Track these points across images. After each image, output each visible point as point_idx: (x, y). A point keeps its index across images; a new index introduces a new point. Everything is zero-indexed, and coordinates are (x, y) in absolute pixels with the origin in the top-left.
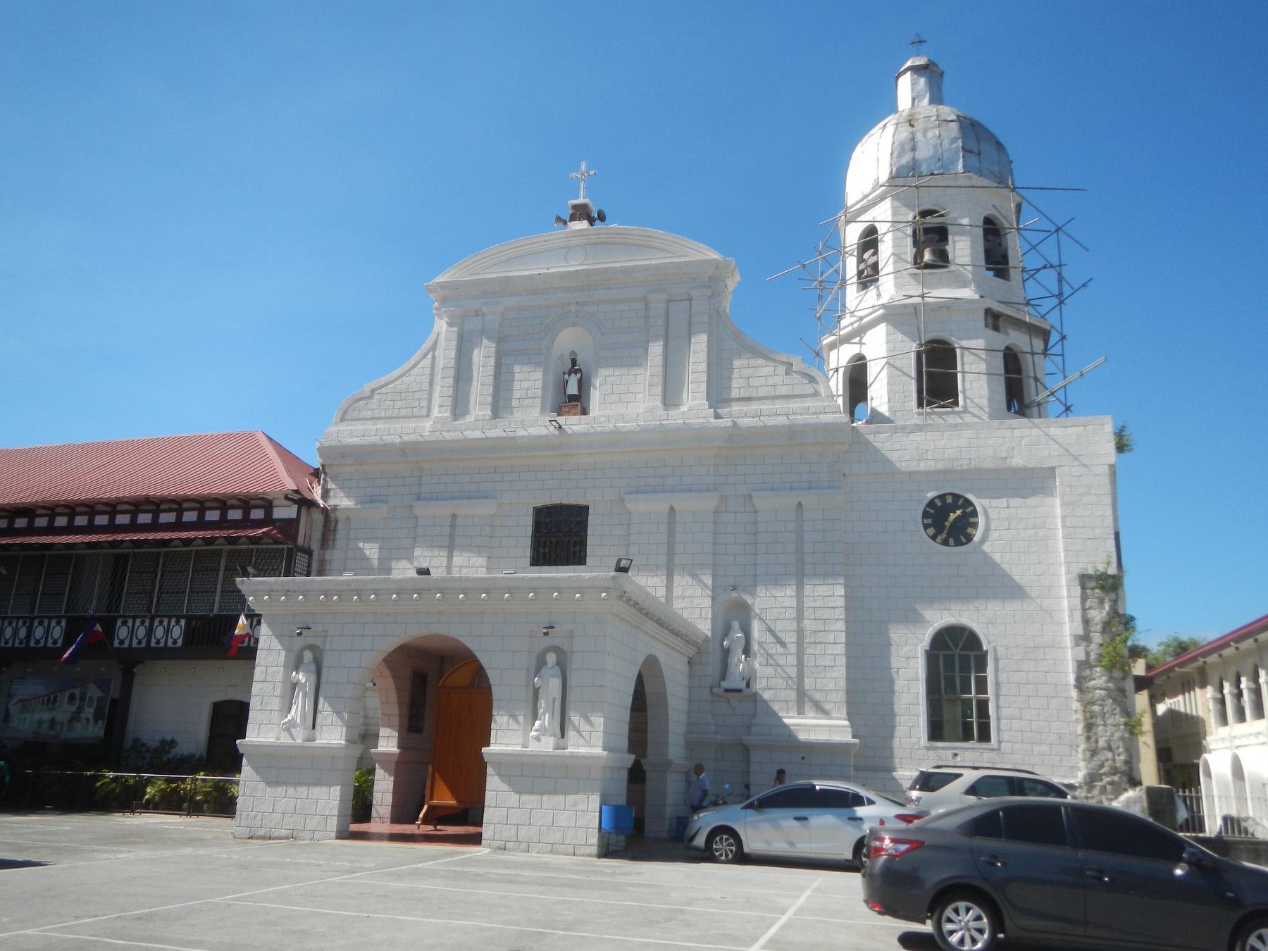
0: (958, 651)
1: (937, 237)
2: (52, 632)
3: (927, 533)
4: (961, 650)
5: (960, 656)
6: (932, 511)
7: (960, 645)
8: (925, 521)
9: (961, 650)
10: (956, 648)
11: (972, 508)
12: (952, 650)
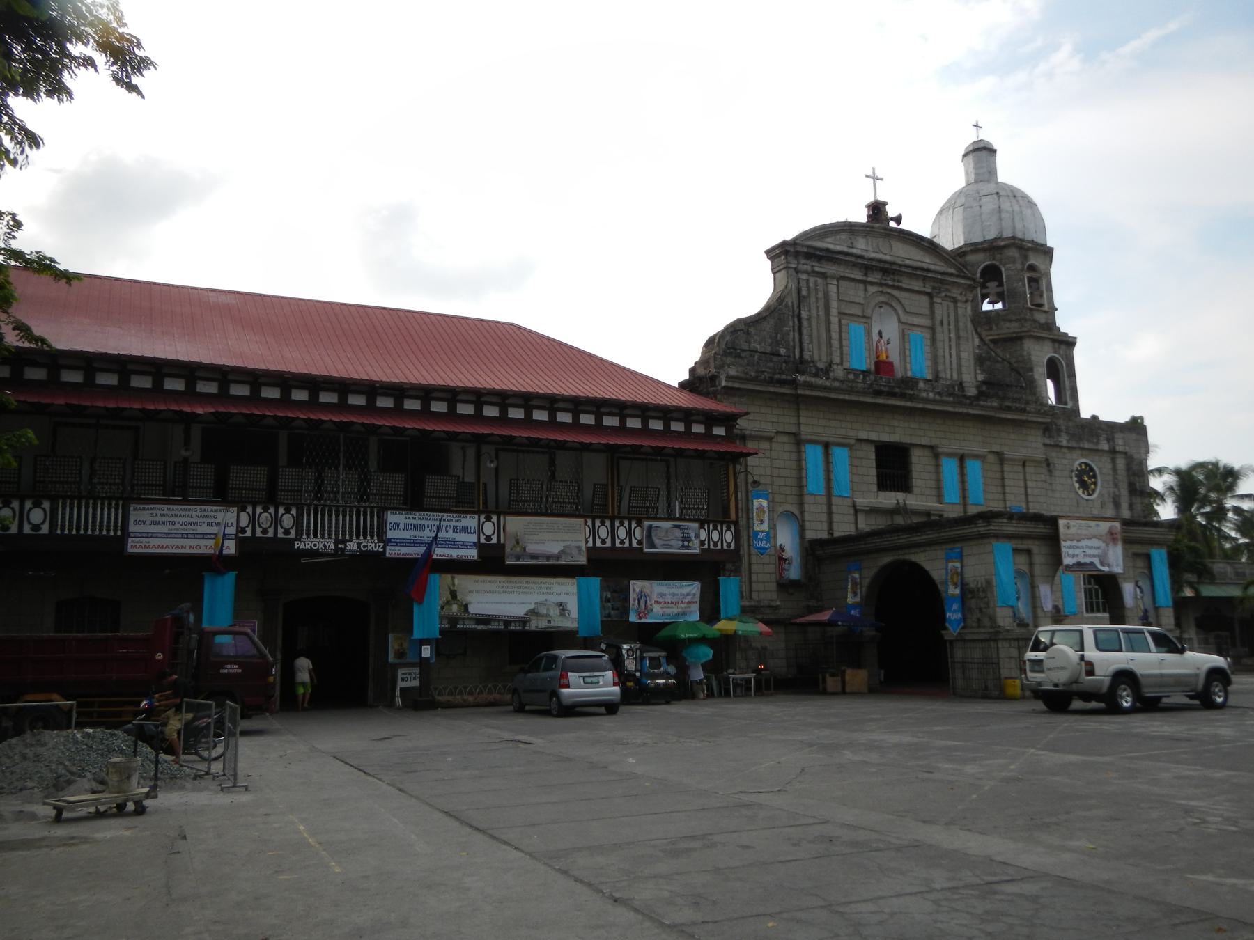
2: (281, 521)
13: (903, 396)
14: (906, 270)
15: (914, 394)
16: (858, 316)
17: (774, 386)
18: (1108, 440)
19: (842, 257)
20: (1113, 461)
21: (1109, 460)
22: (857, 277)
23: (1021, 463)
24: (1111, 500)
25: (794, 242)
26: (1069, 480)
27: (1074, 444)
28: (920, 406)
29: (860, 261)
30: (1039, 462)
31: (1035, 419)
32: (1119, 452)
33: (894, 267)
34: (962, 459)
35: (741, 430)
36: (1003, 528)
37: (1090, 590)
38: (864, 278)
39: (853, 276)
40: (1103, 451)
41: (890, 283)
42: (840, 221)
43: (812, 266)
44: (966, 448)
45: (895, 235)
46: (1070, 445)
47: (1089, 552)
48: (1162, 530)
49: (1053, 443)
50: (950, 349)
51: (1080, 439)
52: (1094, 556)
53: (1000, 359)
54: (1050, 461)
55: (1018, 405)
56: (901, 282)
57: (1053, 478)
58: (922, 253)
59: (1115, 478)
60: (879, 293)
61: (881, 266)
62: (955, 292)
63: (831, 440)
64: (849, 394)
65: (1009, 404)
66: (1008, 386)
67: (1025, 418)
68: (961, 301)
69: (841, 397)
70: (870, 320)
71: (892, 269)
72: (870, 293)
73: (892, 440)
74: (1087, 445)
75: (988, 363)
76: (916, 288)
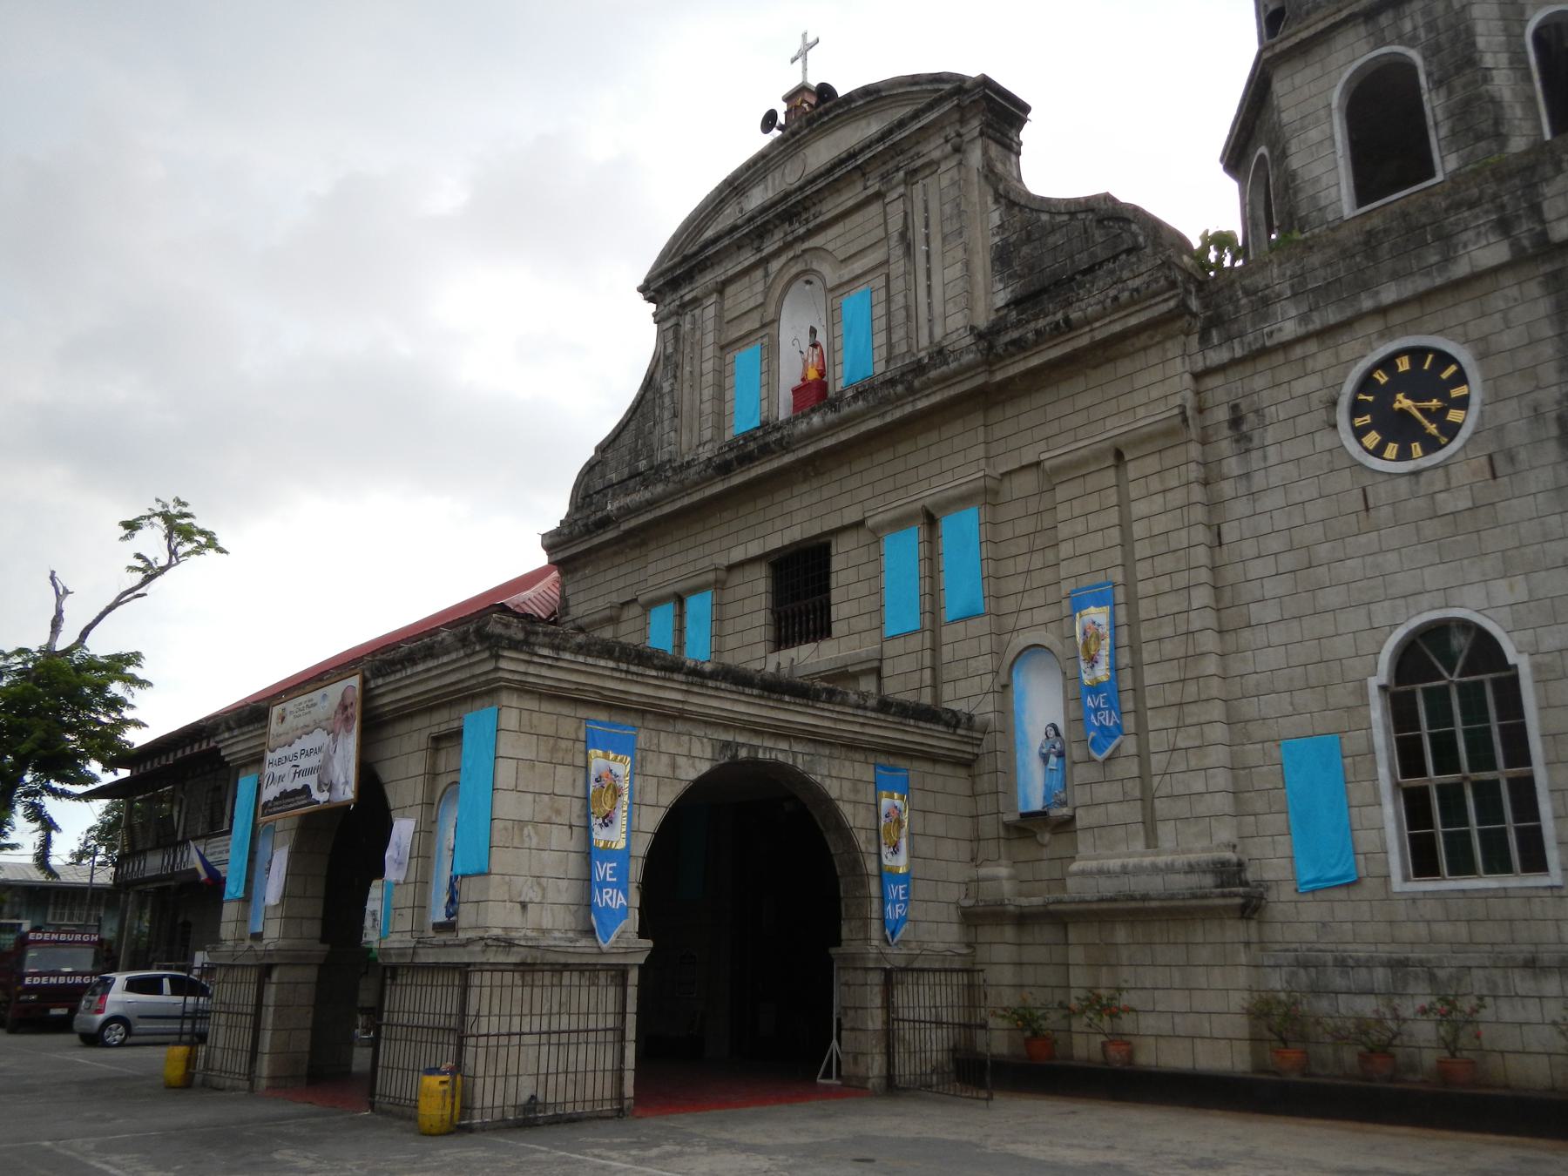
0: (1453, 679)
3: (1361, 443)
4: (1461, 675)
5: (1462, 687)
6: (1370, 398)
7: (1460, 663)
8: (1358, 422)
9: (1461, 675)
10: (1451, 674)
11: (1453, 368)
12: (1443, 678)
13: (766, 451)
14: (815, 189)
15: (782, 438)
16: (756, 330)
17: (598, 535)
18: (1504, 226)
19: (711, 251)
21: (1533, 289)
22: (746, 264)
23: (1111, 461)
24: (1554, 430)
25: (648, 281)
26: (1324, 440)
27: (1332, 316)
28: (810, 450)
29: (737, 235)
30: (1169, 433)
33: (793, 200)
34: (930, 520)
35: (573, 620)
36: (235, 749)
38: (758, 256)
39: (739, 268)
40: (1496, 270)
41: (802, 231)
42: (708, 192)
43: (682, 297)
44: (927, 494)
45: (805, 136)
46: (1317, 323)
47: (304, 763)
48: (454, 656)
49: (1239, 353)
50: (929, 277)
51: (1366, 286)
53: (1065, 218)
54: (1244, 407)
55: (1041, 323)
56: (821, 214)
57: (1255, 455)
58: (863, 123)
60: (791, 263)
61: (771, 215)
62: (934, 148)
63: (678, 587)
64: (688, 495)
65: (1015, 334)
66: (1084, 272)
67: (1084, 341)
68: (946, 158)
69: (678, 505)
70: (776, 325)
71: (793, 205)
72: (772, 276)
74: (1389, 294)
75: (1025, 250)
76: (850, 203)
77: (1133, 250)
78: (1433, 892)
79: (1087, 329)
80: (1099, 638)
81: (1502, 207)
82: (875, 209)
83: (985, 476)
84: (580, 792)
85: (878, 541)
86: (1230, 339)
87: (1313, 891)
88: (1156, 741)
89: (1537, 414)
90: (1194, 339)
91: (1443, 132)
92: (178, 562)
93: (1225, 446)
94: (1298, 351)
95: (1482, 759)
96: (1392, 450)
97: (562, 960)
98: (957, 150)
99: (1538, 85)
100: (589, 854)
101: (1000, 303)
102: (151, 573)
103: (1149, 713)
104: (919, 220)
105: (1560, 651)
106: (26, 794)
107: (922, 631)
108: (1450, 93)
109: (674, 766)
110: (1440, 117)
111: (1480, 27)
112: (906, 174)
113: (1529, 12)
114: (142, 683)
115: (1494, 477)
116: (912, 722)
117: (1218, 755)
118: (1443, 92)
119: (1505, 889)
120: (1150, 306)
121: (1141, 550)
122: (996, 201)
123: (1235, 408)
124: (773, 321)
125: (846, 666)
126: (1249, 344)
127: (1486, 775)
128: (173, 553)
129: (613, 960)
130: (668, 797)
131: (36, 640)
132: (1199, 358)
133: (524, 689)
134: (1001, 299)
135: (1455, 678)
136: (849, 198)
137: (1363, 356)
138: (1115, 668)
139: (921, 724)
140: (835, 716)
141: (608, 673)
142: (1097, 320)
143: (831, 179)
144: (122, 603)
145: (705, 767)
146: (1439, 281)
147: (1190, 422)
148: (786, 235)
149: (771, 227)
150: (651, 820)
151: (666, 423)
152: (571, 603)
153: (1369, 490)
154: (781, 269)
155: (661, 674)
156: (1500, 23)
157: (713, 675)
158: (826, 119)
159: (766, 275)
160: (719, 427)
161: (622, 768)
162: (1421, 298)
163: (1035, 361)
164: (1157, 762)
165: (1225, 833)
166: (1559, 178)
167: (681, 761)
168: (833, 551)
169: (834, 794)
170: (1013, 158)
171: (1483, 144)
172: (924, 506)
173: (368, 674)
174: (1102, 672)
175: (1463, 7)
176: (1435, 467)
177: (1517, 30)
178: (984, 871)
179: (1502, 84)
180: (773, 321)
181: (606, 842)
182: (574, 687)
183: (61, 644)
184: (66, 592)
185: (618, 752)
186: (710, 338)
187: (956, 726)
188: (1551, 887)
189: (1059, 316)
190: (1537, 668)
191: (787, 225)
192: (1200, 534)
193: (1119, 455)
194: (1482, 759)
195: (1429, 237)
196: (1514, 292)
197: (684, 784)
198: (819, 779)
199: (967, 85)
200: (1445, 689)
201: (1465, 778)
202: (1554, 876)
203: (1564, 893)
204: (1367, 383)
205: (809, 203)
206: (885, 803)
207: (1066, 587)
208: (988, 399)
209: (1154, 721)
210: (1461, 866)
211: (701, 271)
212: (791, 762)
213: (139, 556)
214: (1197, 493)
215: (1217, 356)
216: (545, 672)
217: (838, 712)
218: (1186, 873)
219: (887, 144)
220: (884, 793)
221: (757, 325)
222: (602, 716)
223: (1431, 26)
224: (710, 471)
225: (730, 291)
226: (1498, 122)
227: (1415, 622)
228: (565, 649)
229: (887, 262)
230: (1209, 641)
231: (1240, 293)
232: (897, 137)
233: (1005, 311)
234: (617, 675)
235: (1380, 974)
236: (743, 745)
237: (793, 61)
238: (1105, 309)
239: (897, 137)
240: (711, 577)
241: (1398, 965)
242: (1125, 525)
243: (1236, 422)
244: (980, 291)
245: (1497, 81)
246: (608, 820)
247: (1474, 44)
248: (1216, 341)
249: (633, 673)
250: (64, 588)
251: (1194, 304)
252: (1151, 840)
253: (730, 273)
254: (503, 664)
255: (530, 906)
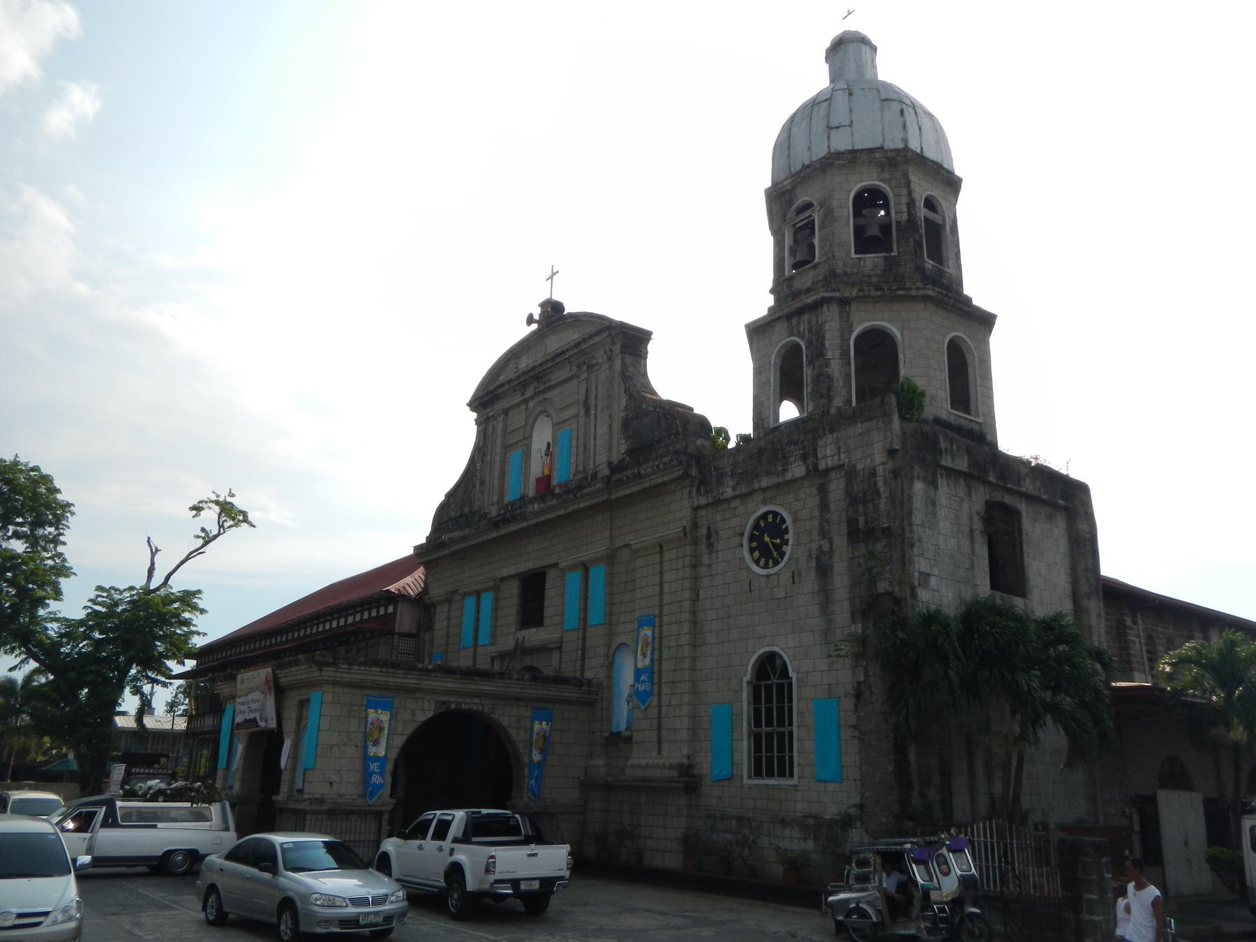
1: (808, 232)
3: (752, 556)
4: (778, 679)
6: (757, 533)
18: (804, 457)
19: (500, 391)
20: (823, 490)
21: (814, 491)
23: (658, 549)
24: (814, 564)
27: (743, 489)
28: (534, 521)
31: (660, 481)
32: (827, 471)
34: (586, 569)
37: (769, 736)
39: (514, 402)
41: (542, 388)
46: (738, 493)
51: (756, 476)
52: (255, 711)
57: (714, 555)
59: (823, 520)
67: (647, 485)
73: (526, 569)
74: (764, 483)
76: (564, 377)
77: (677, 434)
78: (758, 785)
79: (648, 479)
80: (647, 644)
81: (804, 448)
82: (574, 383)
83: (606, 549)
84: (362, 730)
85: (564, 575)
86: (707, 492)
87: (717, 781)
88: (665, 700)
89: (810, 556)
90: (694, 490)
91: (809, 390)
92: (224, 532)
93: (704, 549)
94: (733, 504)
95: (781, 724)
96: (762, 561)
97: (349, 808)
98: (609, 359)
99: (853, 368)
100: (366, 759)
101: (623, 451)
102: (208, 539)
103: (663, 685)
104: (593, 397)
105: (807, 672)
106: (132, 681)
107: (579, 629)
108: (813, 370)
109: (413, 715)
110: (809, 381)
111: (828, 335)
112: (588, 367)
113: (855, 326)
114: (202, 611)
115: (794, 583)
116: (553, 685)
117: (685, 710)
118: (811, 367)
119: (780, 785)
120: (672, 472)
121: (666, 599)
122: (625, 392)
123: (709, 528)
124: (529, 437)
125: (546, 644)
126: (714, 497)
127: (781, 729)
128: (221, 526)
129: (375, 809)
130: (409, 730)
131: (140, 582)
132: (696, 499)
133: (334, 683)
134: (623, 448)
135: (775, 681)
136: (563, 374)
137: (755, 512)
138: (652, 660)
139: (559, 686)
140: (505, 685)
141: (377, 673)
142: (652, 475)
143: (554, 363)
144: (190, 558)
145: (430, 714)
146: (781, 480)
147: (688, 534)
148: (536, 388)
149: (528, 382)
150: (399, 742)
151: (477, 488)
152: (429, 587)
153: (752, 581)
154: (534, 407)
155: (405, 672)
156: (839, 332)
157: (433, 670)
158: (554, 325)
159: (527, 409)
160: (501, 495)
161: (385, 717)
162: (777, 486)
163: (628, 492)
164: (664, 709)
165: (685, 751)
166: (824, 438)
167: (418, 712)
168: (547, 578)
169: (505, 724)
170: (642, 361)
171: (821, 400)
172: (582, 561)
173: (274, 668)
174: (647, 661)
175: (822, 323)
176: (774, 574)
177: (847, 337)
178: (594, 762)
179: (835, 368)
180: (529, 437)
181: (375, 753)
182: (359, 681)
183: (153, 586)
184: (157, 550)
185: (383, 709)
186: (499, 441)
187: (581, 685)
188: (794, 785)
189: (636, 470)
190: (799, 680)
191: (536, 382)
192: (687, 595)
193: (661, 547)
194: (781, 724)
195: (779, 456)
196: (807, 490)
197: (418, 723)
198: (497, 717)
199: (613, 325)
200: (772, 685)
201: (774, 730)
202: (795, 781)
203: (798, 788)
204: (756, 526)
205: (545, 373)
206: (537, 726)
207: (638, 613)
208: (610, 506)
209: (666, 690)
210: (770, 774)
211: (498, 399)
212: (480, 709)
213: (203, 530)
214: (688, 572)
215: (703, 501)
216: (344, 675)
217: (507, 683)
218: (669, 769)
219: (580, 349)
220: (537, 722)
221: (521, 438)
222: (376, 693)
223: (810, 332)
224: (490, 525)
225: (511, 414)
226: (829, 389)
227: (762, 651)
228: (354, 665)
229: (577, 416)
230: (687, 651)
231: (713, 469)
232: (584, 346)
233: (624, 456)
234: (381, 674)
235: (734, 823)
236: (453, 702)
237: (547, 279)
238: (654, 470)
239: (584, 346)
240: (491, 584)
241: (740, 819)
242: (661, 584)
243: (709, 536)
244: (615, 443)
245: (832, 366)
246: (376, 743)
247: (824, 344)
248: (702, 492)
249: (390, 673)
250: (156, 548)
251: (694, 472)
252: (659, 752)
253: (510, 404)
254: (323, 673)
255: (334, 784)
